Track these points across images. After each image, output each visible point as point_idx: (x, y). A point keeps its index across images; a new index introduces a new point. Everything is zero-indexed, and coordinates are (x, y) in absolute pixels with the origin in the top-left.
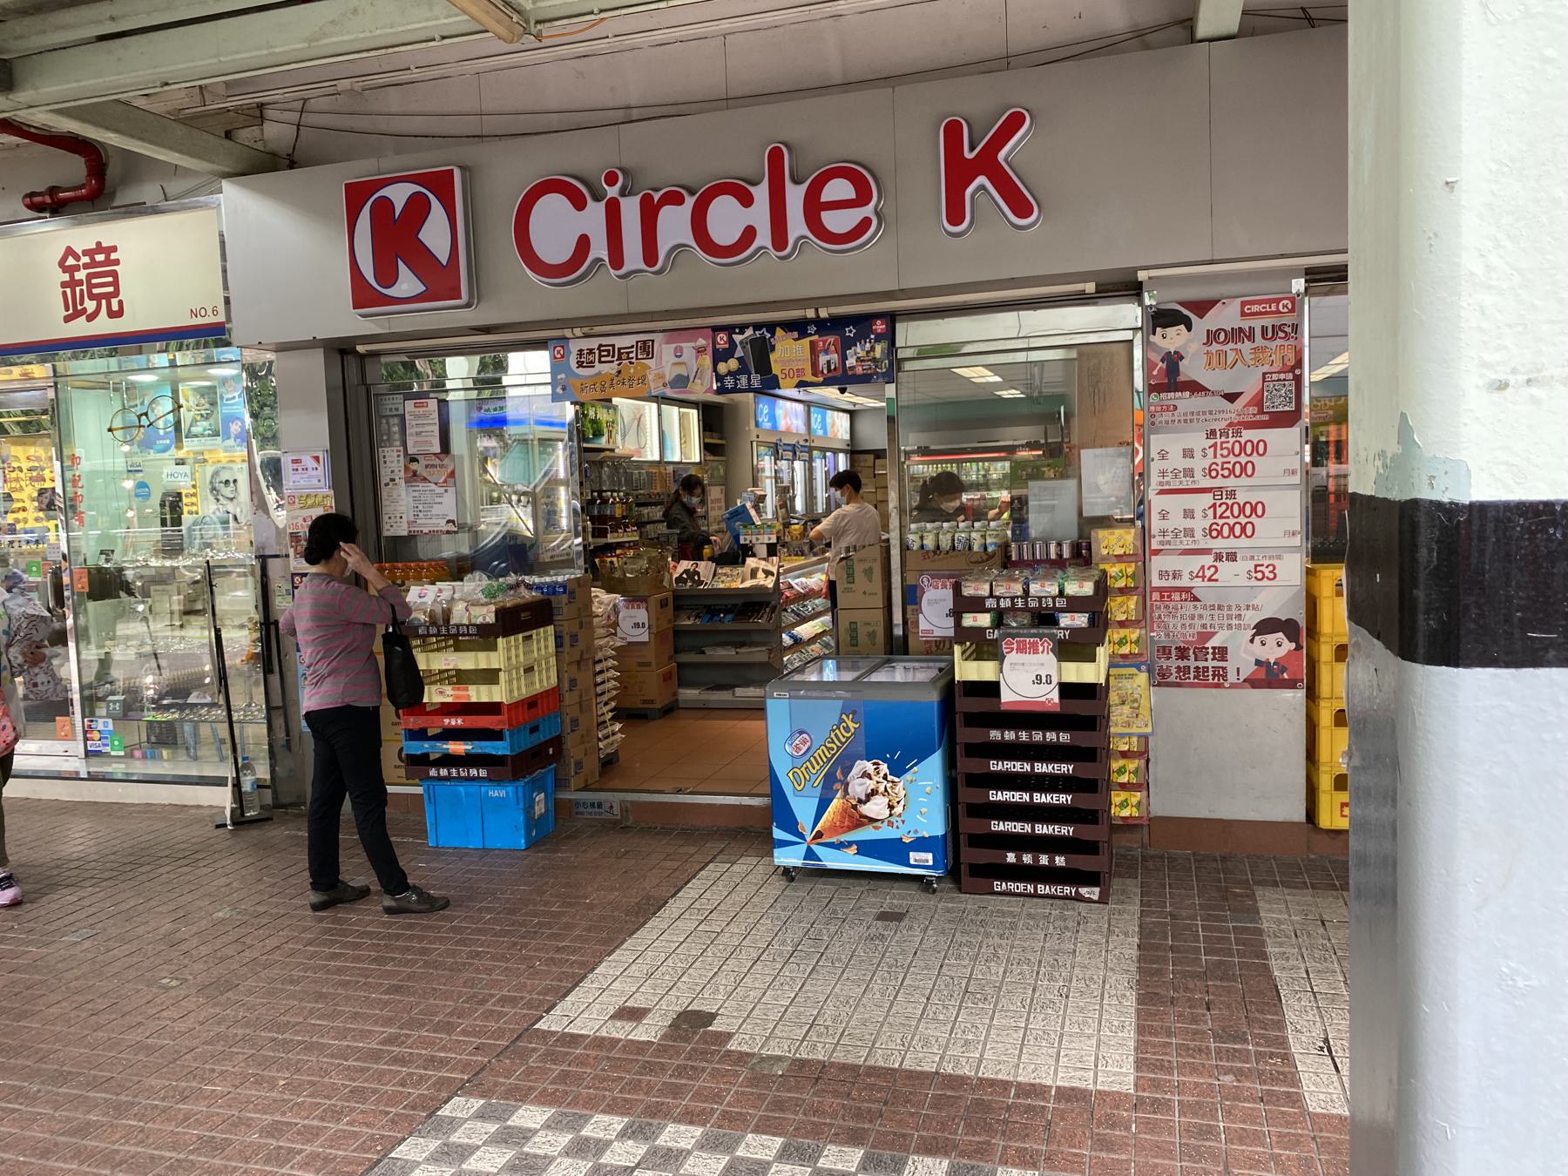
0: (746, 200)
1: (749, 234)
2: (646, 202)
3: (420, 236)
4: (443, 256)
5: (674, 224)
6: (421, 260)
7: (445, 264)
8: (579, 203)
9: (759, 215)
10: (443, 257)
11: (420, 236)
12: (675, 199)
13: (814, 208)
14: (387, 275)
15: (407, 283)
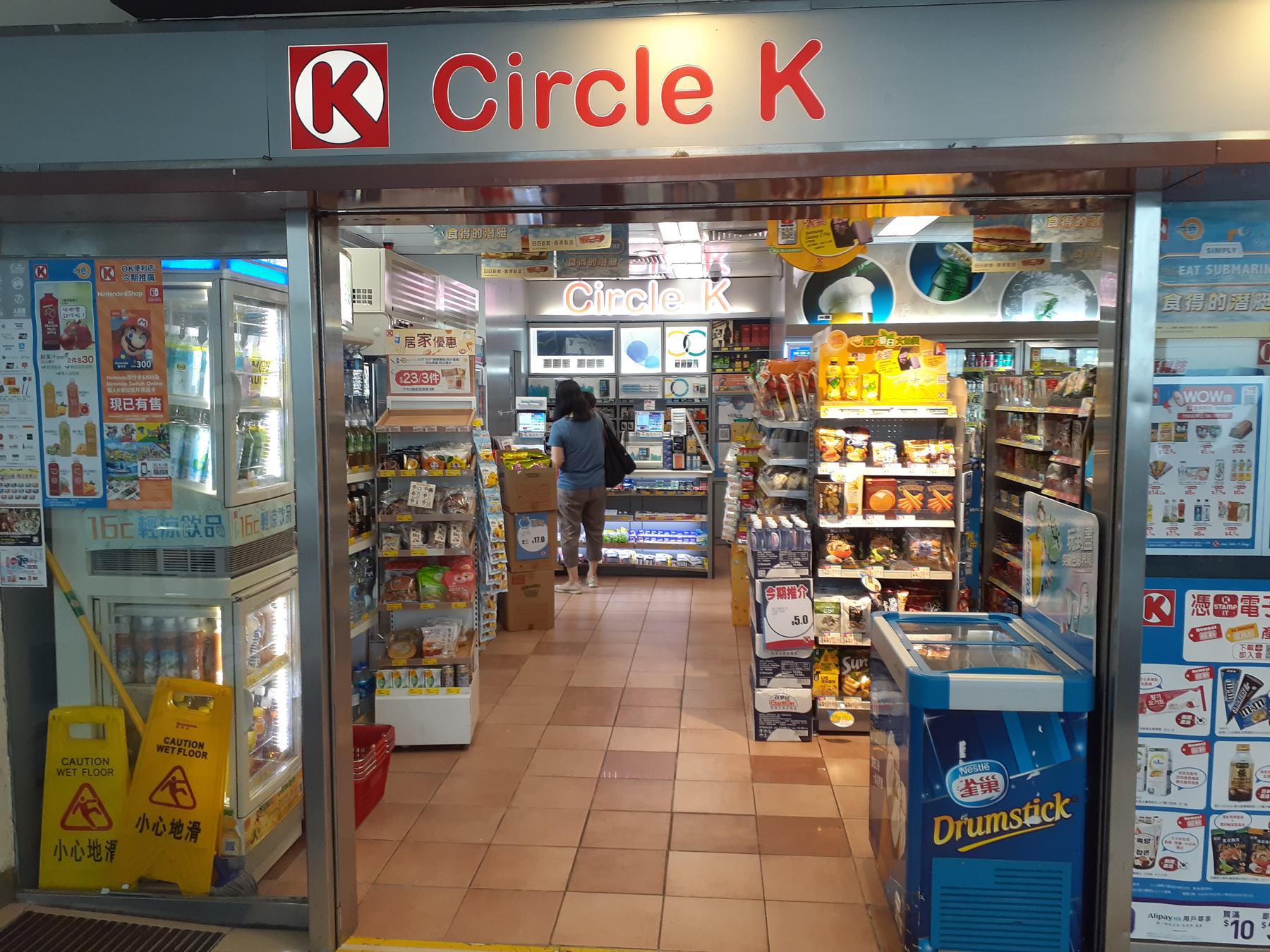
0: (618, 83)
1: (620, 111)
2: (542, 77)
3: (355, 95)
4: (375, 114)
5: (564, 97)
6: (356, 115)
7: (376, 120)
8: (490, 75)
9: (629, 96)
10: (375, 114)
11: (355, 95)
12: (564, 78)
13: (670, 95)
14: (324, 123)
15: (342, 131)
